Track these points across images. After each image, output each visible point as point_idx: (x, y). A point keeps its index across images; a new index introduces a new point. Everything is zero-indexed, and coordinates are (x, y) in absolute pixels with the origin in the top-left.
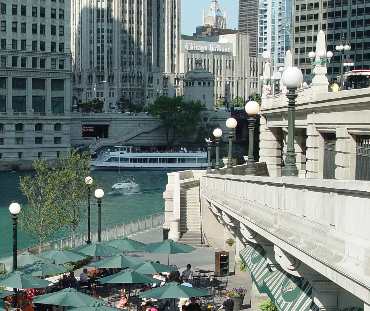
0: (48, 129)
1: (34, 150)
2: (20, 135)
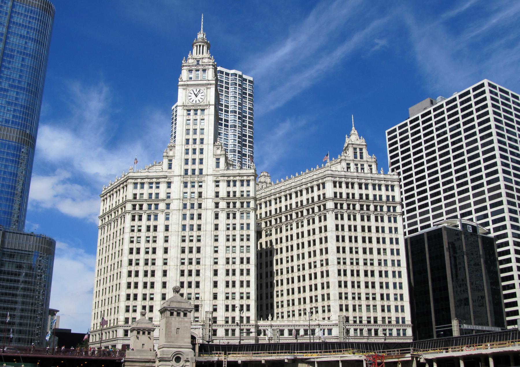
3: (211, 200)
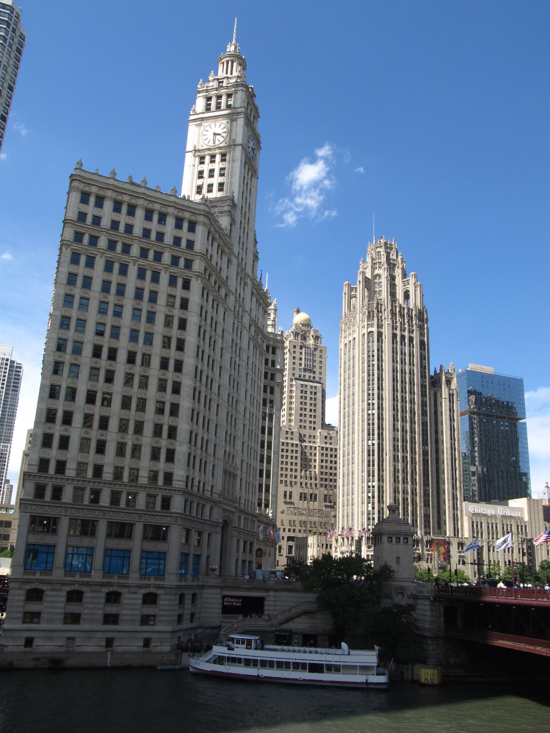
0: (131, 601)
1: (99, 635)
2: (74, 608)
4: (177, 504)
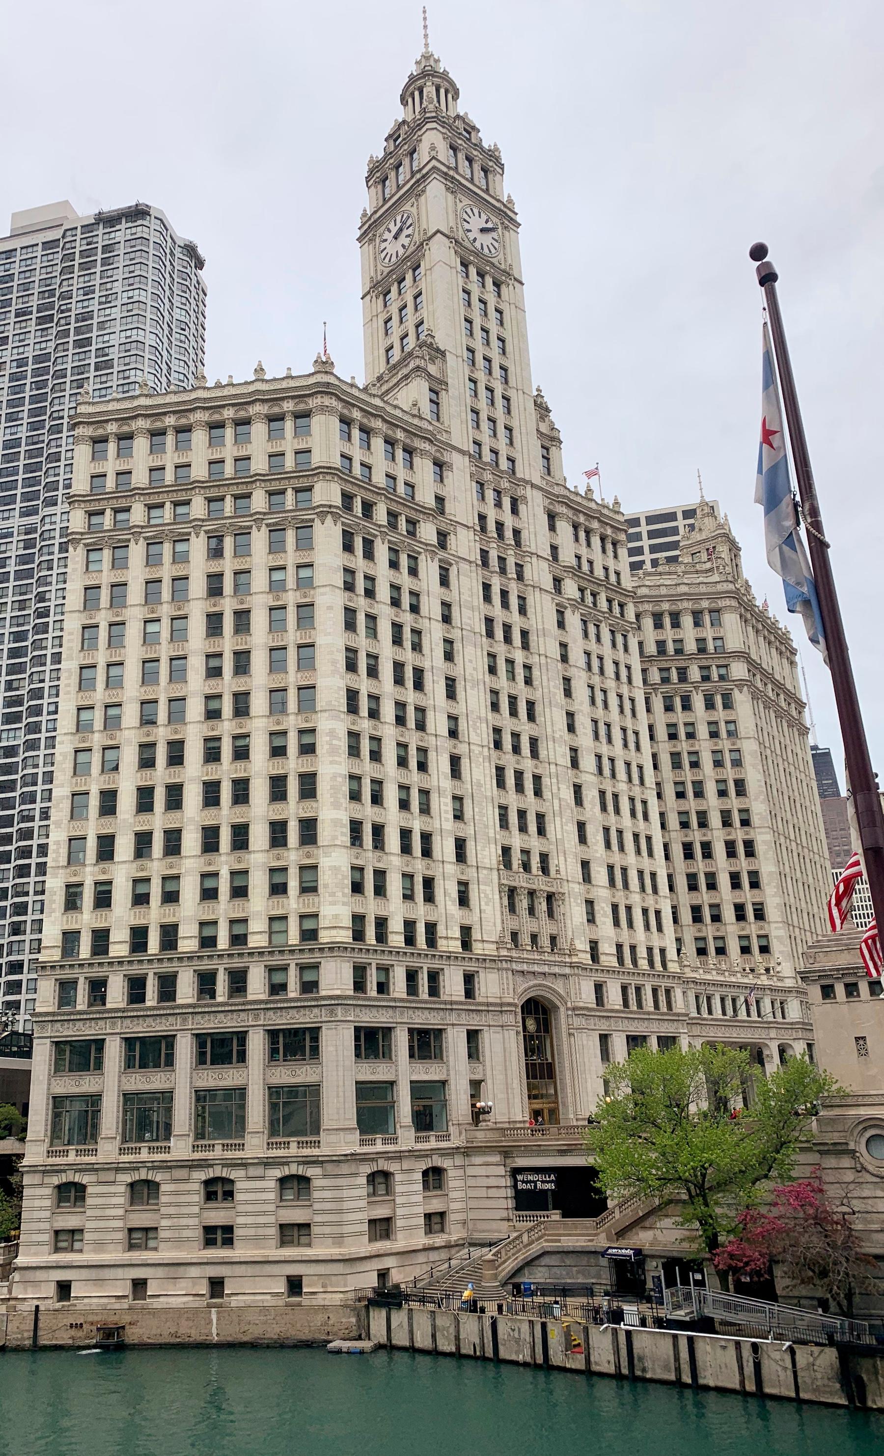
1: (194, 1272)
3: (545, 565)
4: (336, 977)
